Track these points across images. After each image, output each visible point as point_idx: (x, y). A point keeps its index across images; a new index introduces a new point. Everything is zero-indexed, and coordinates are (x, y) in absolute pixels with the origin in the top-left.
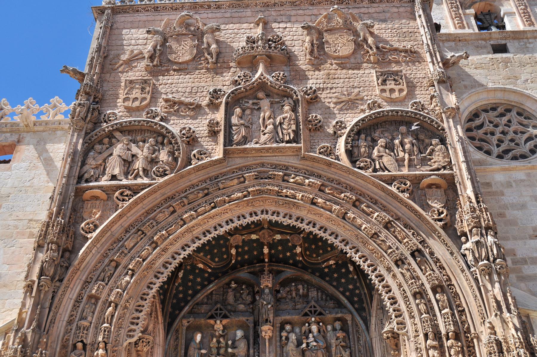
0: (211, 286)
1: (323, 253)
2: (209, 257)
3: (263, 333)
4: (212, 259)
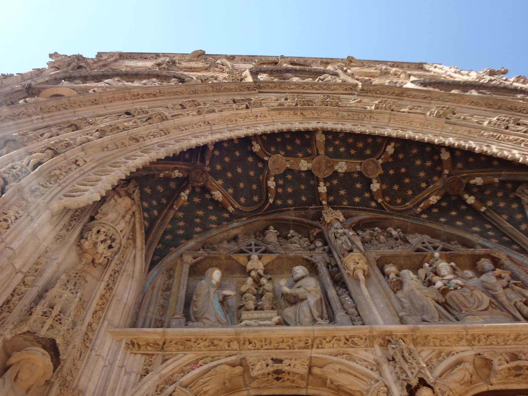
0: (235, 224)
1: (414, 194)
2: (231, 191)
3: (352, 266)
4: (236, 197)
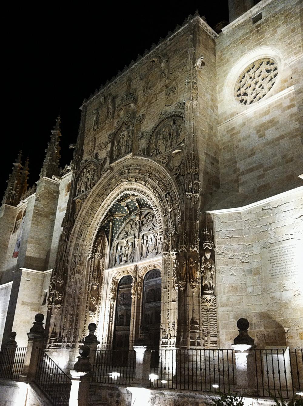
2: (120, 213)
